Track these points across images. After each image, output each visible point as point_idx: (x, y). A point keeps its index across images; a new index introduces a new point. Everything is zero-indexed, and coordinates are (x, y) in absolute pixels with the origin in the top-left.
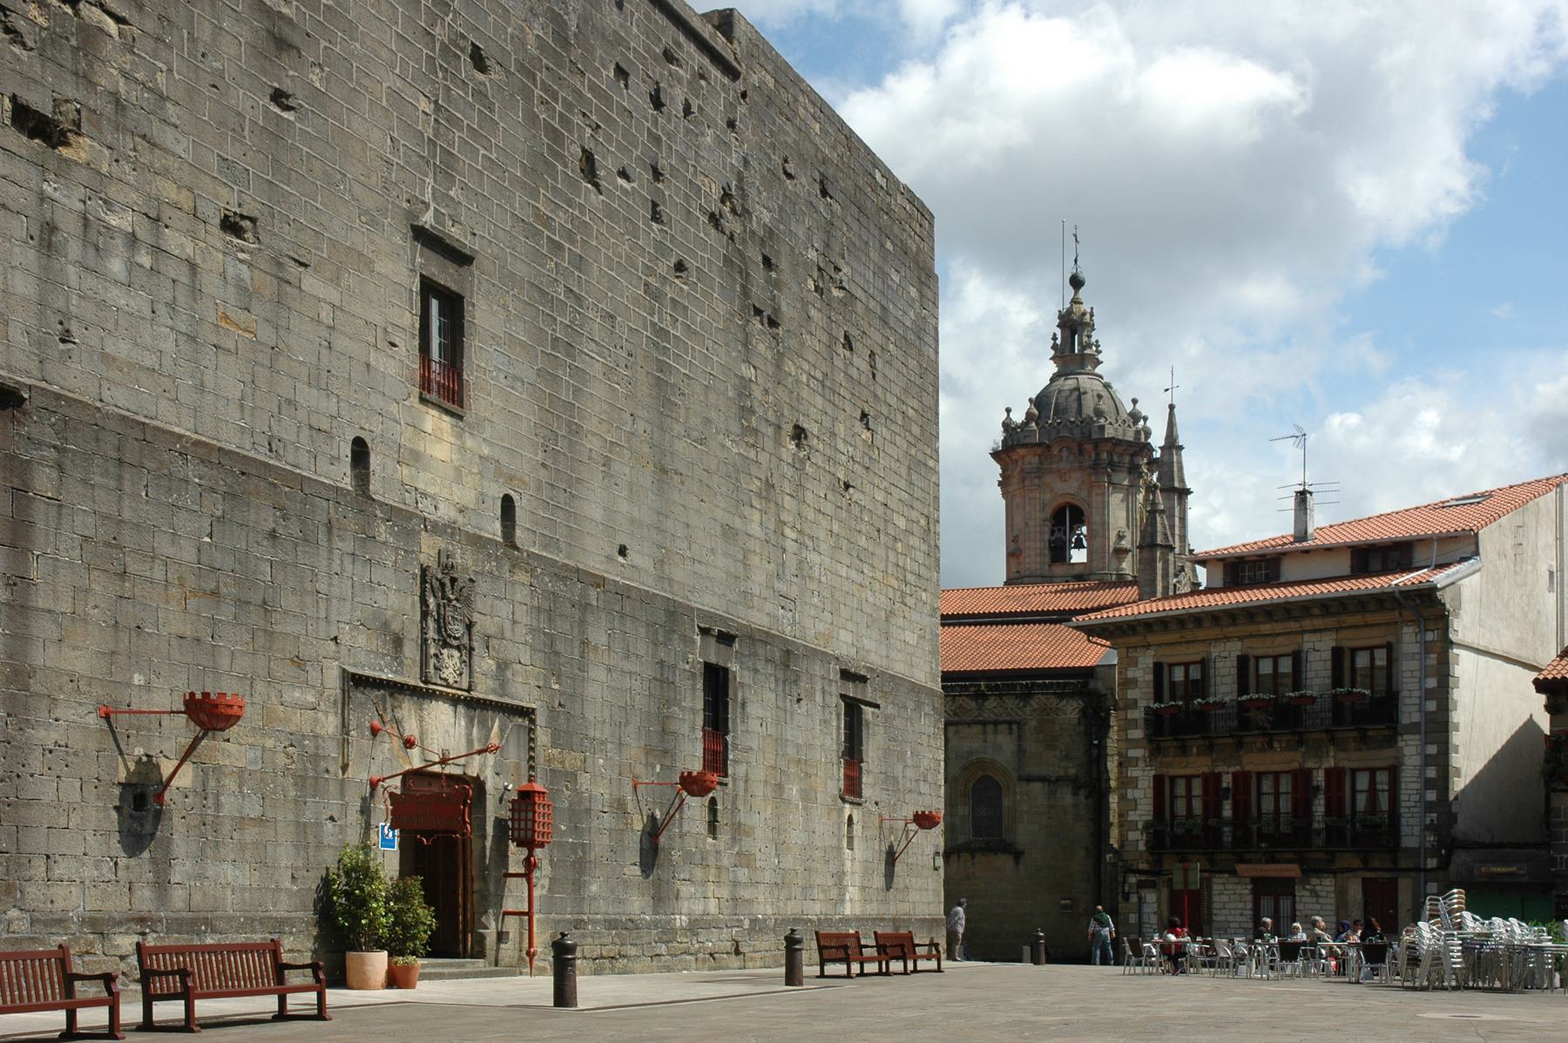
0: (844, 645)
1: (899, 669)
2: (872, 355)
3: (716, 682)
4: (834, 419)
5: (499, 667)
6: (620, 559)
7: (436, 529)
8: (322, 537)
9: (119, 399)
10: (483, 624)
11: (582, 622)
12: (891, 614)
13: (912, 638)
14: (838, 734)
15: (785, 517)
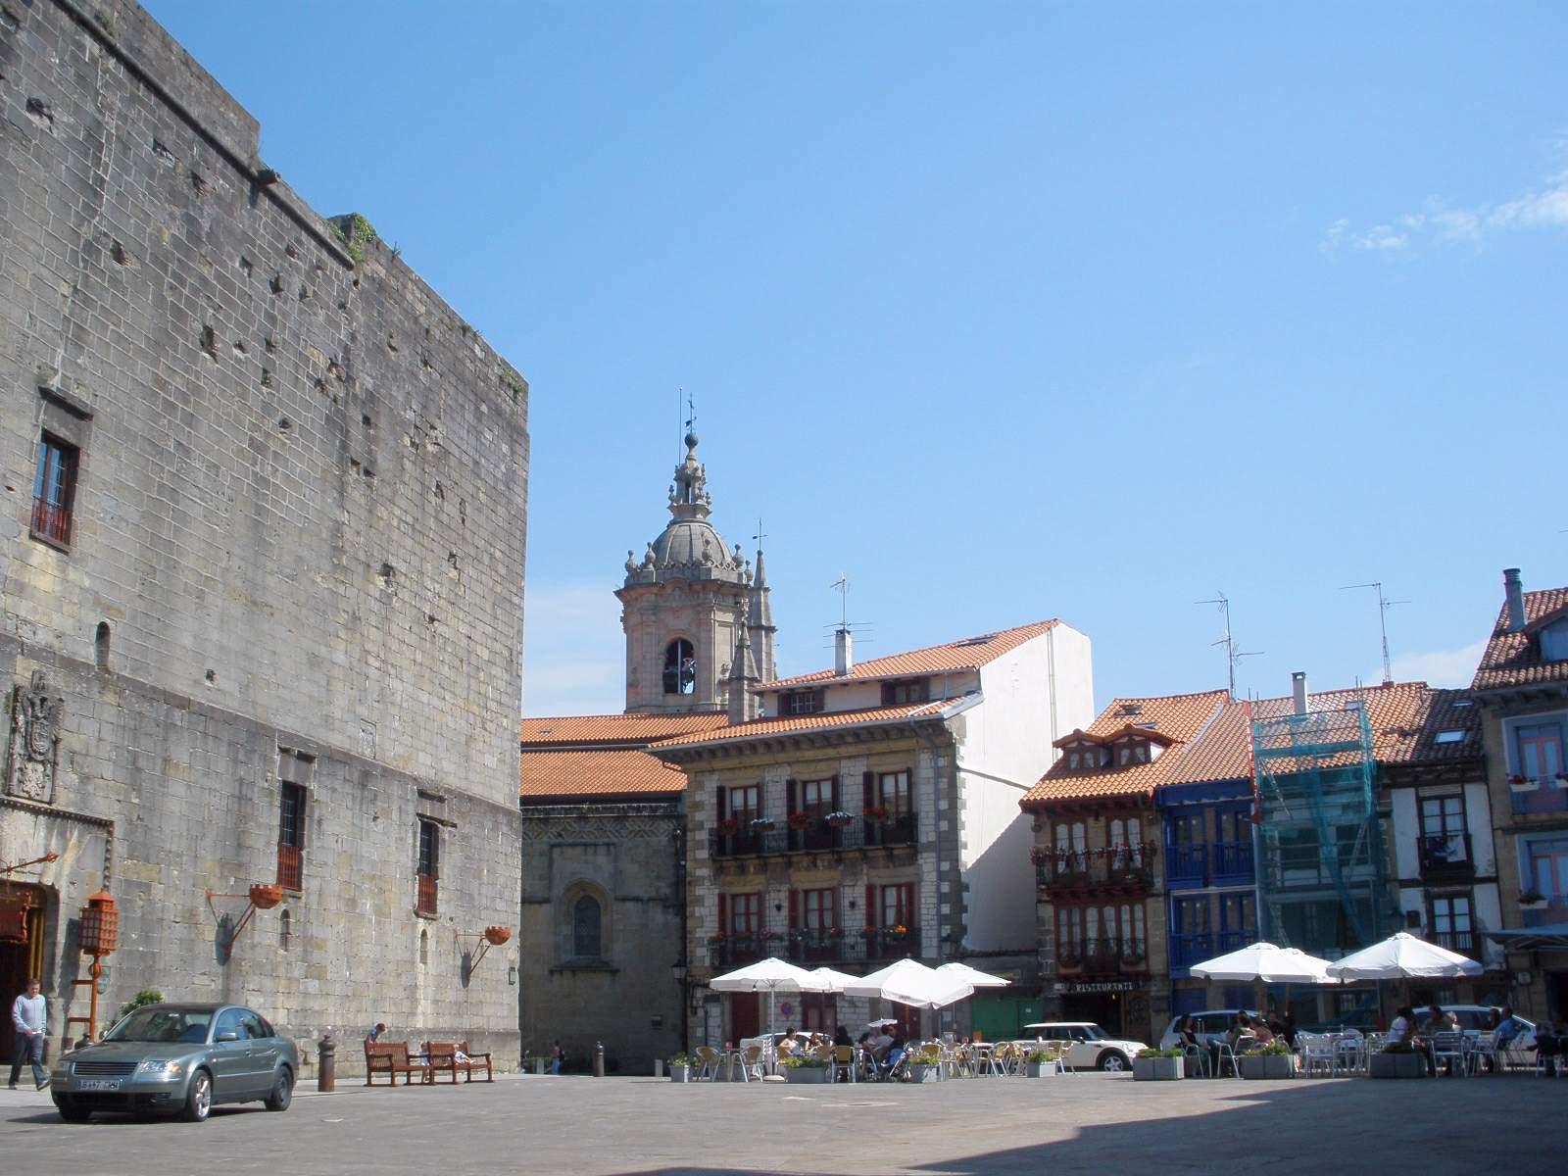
0: (423, 767)
1: (477, 790)
2: (462, 502)
3: (294, 798)
4: (422, 559)
5: (82, 781)
6: (208, 683)
7: (33, 653)
10: (70, 741)
11: (165, 740)
12: (470, 738)
13: (491, 761)
15: (368, 646)
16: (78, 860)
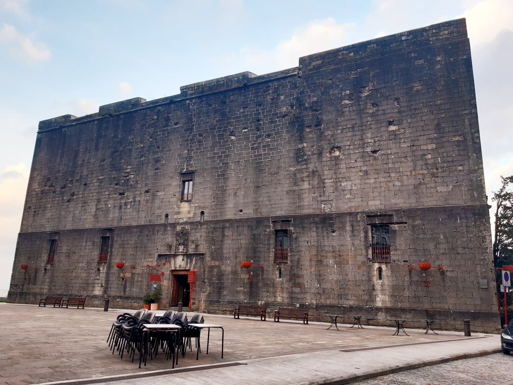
8: (156, 233)
9: (127, 224)
14: (366, 237)
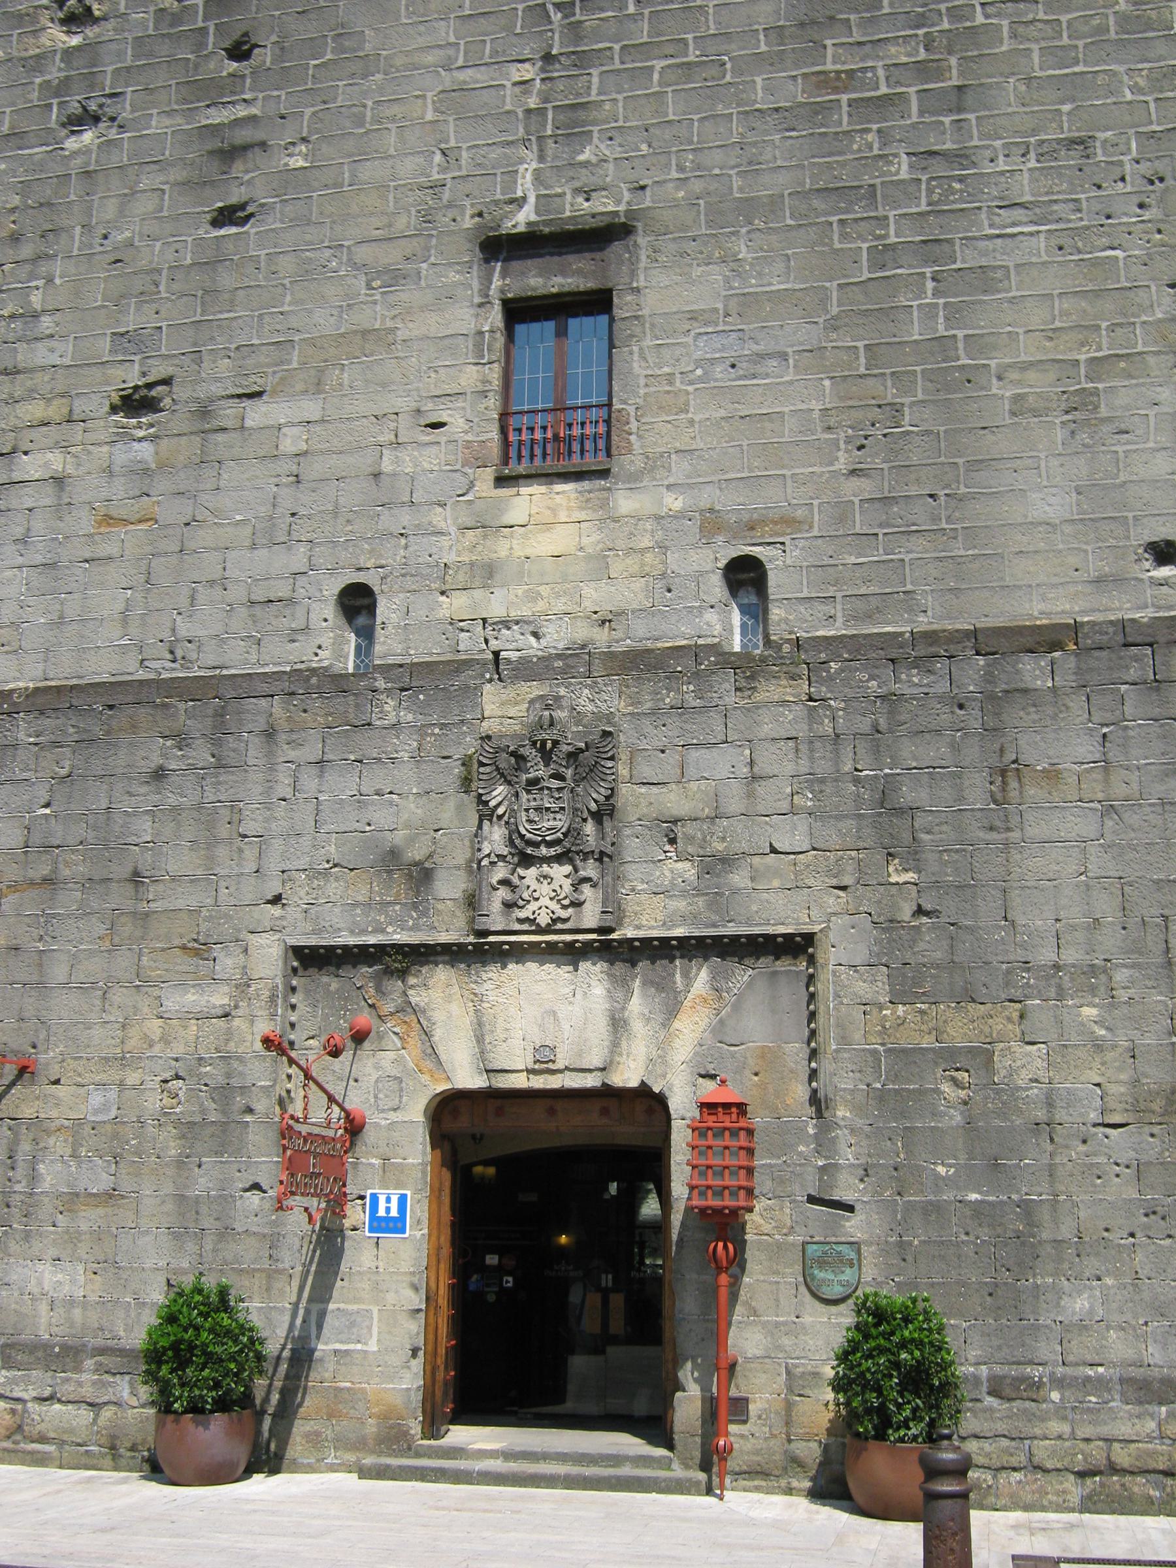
11: (993, 731)
16: (719, 1029)
